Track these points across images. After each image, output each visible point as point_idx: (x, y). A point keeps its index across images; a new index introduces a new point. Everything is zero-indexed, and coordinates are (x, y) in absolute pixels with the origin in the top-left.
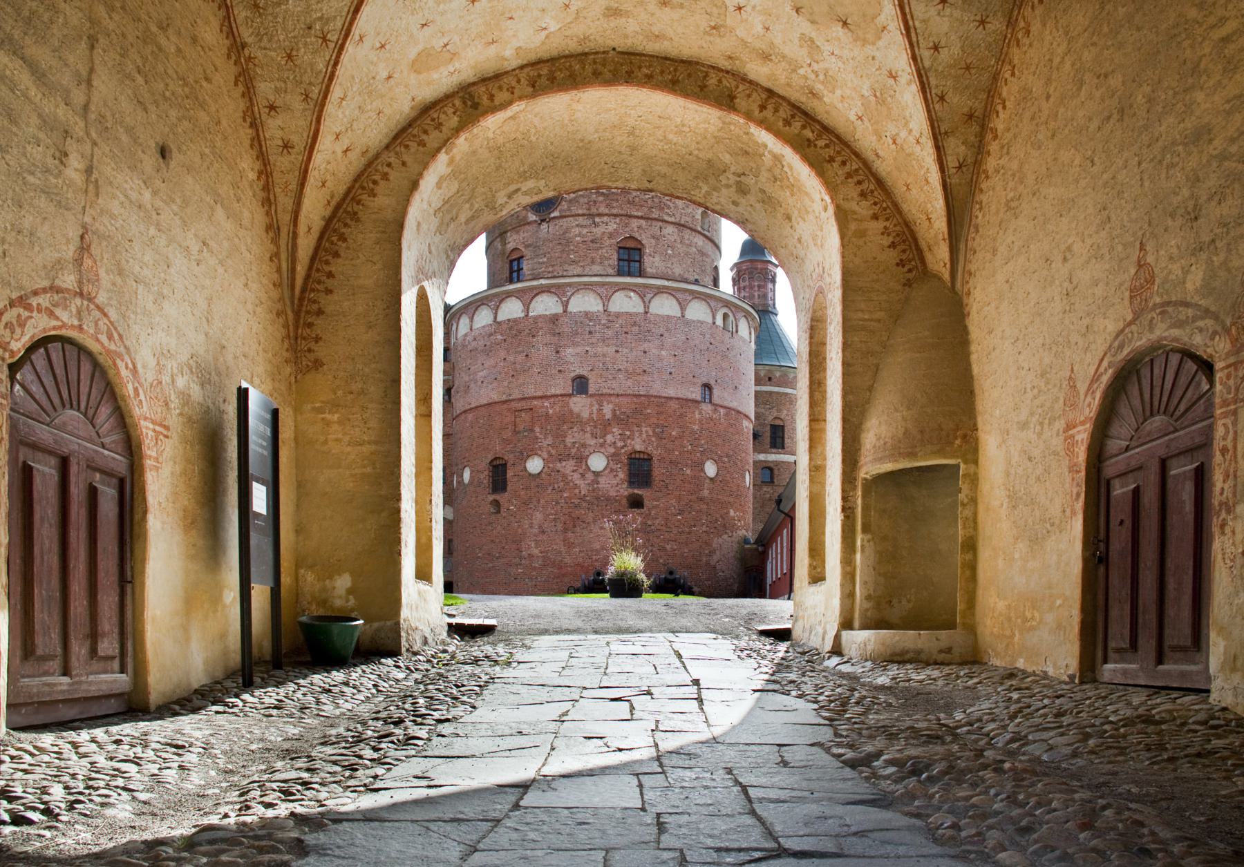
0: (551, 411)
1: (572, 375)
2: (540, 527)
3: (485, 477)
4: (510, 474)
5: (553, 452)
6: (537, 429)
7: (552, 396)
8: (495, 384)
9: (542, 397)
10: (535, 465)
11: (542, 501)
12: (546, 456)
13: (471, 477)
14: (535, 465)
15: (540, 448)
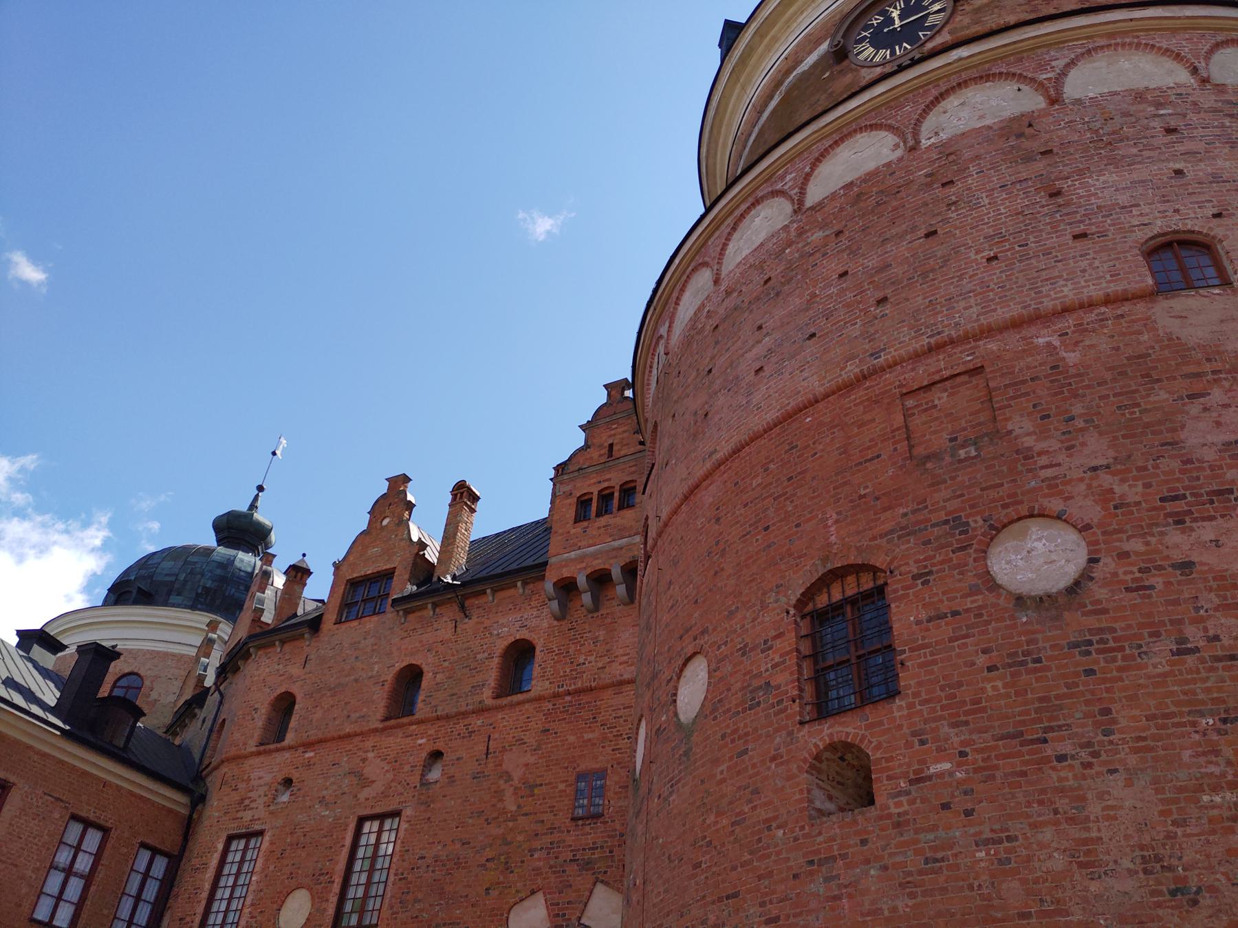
0: (1072, 357)
1: (1141, 235)
2: (1151, 863)
3: (781, 665)
4: (905, 618)
5: (1131, 491)
6: (1020, 425)
7: (1066, 310)
8: (812, 347)
9: (1016, 324)
10: (1037, 559)
11: (1124, 717)
12: (1091, 511)
13: (711, 707)
14: (1037, 559)
15: (1054, 486)
